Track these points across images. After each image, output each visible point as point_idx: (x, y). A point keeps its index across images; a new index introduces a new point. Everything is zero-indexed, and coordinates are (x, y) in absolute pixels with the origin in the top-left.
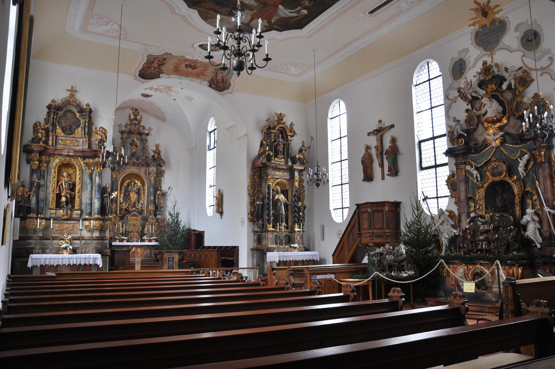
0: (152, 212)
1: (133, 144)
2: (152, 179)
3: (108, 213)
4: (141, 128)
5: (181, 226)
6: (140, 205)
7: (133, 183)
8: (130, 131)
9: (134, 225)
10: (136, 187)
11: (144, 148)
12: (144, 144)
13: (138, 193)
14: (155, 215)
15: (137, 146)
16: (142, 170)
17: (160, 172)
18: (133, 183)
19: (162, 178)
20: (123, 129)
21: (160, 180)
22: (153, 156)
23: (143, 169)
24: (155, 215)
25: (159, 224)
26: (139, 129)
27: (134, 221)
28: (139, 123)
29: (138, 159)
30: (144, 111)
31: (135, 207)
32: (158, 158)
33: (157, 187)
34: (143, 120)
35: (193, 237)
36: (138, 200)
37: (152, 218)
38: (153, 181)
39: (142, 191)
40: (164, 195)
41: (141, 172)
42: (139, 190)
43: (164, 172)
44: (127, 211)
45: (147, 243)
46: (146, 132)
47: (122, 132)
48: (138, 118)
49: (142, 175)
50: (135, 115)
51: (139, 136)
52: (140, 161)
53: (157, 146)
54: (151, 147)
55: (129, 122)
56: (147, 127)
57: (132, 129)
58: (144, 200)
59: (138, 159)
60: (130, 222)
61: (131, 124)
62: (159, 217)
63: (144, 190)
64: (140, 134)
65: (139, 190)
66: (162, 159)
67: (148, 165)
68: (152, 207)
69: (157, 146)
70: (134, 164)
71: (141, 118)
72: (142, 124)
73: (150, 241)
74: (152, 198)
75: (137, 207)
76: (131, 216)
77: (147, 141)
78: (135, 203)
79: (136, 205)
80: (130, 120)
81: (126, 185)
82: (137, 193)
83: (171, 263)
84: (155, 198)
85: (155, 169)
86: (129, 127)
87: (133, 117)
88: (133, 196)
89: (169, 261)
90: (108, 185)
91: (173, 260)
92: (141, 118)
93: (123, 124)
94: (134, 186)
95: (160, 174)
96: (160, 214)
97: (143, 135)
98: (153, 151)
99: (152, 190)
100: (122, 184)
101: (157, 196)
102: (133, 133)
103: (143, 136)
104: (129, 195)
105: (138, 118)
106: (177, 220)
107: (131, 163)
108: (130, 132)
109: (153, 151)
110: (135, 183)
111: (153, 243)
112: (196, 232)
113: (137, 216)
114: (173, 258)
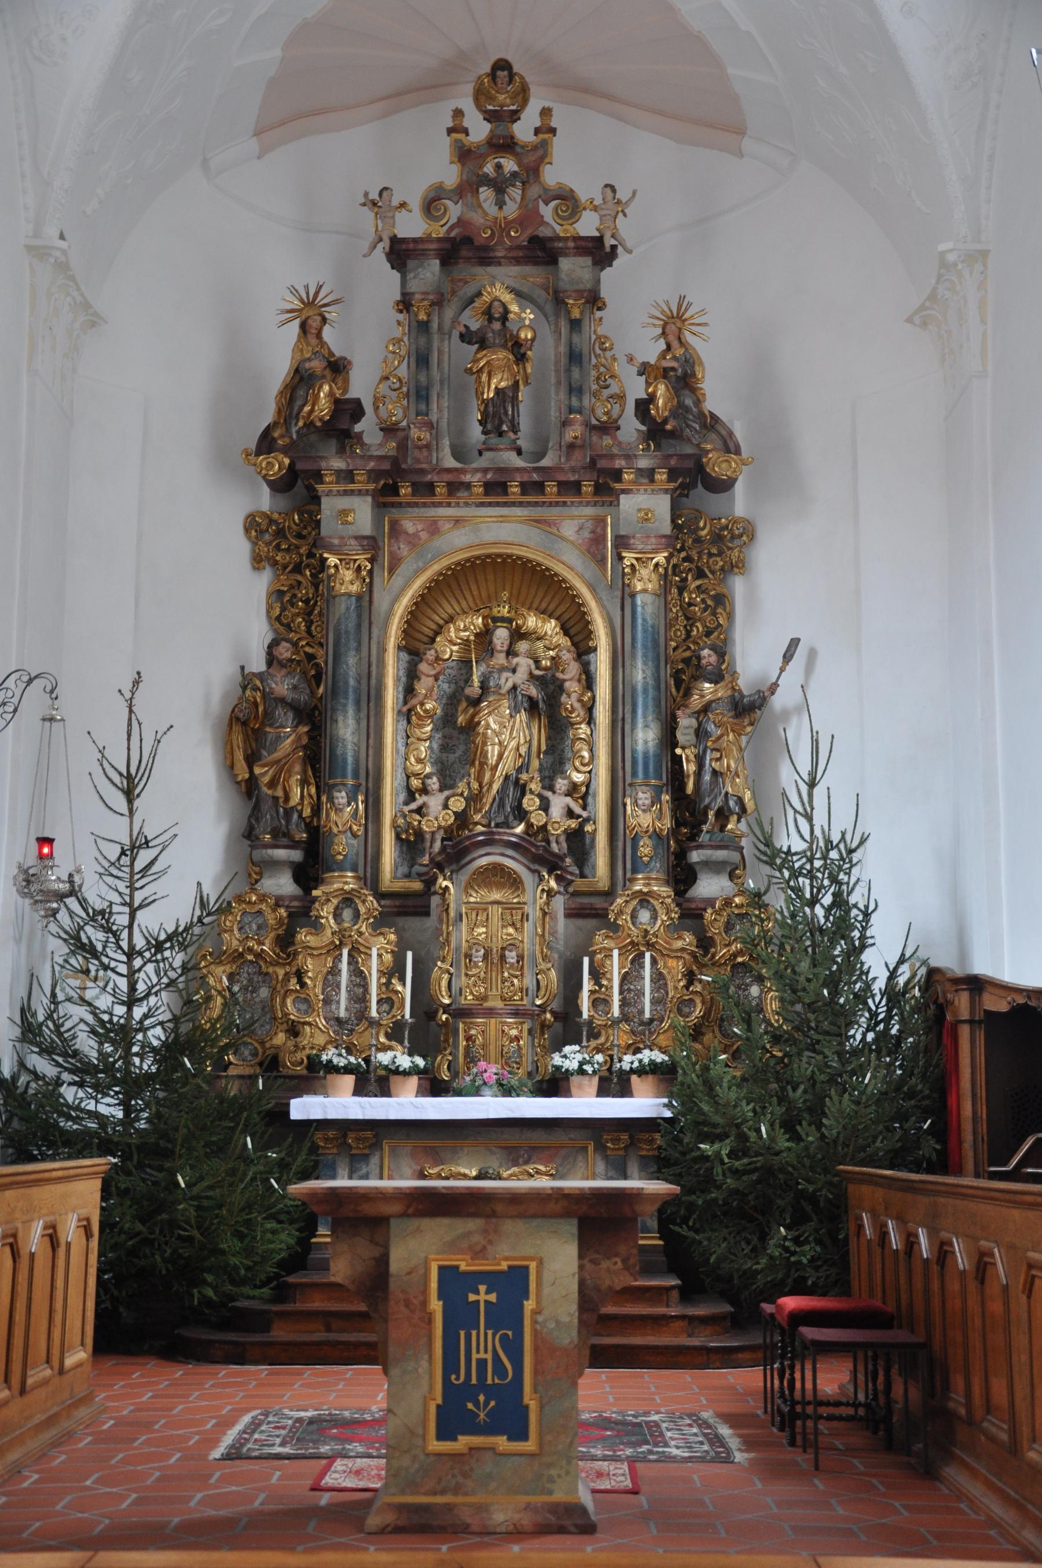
0: (645, 848)
1: (494, 332)
2: (645, 582)
4: (547, 211)
5: (876, 963)
6: (559, 804)
7: (501, 636)
8: (467, 240)
9: (495, 958)
10: (524, 663)
11: (575, 357)
12: (575, 325)
13: (546, 705)
14: (682, 876)
15: (518, 351)
16: (568, 529)
17: (717, 538)
18: (501, 636)
19: (738, 586)
20: (412, 225)
21: (721, 600)
22: (643, 407)
23: (573, 522)
24: (682, 876)
25: (705, 943)
26: (529, 216)
27: (499, 928)
28: (531, 173)
30: (584, 91)
31: (521, 814)
32: (679, 411)
33: (690, 656)
34: (558, 145)
35: (969, 1053)
36: (555, 756)
37: (644, 900)
38: (646, 605)
39: (571, 701)
40: (748, 708)
41: (558, 540)
43: (747, 532)
44: (456, 849)
45: (584, 1104)
46: (587, 225)
47: (401, 254)
48: (524, 130)
49: (570, 565)
50: (491, 117)
51: (533, 275)
52: (546, 462)
53: (674, 324)
54: (629, 332)
55: (450, 175)
56: (587, 190)
57: (477, 219)
58: (593, 762)
60: (461, 935)
61: (467, 189)
62: (710, 887)
63: (589, 682)
64: (542, 252)
66: (711, 423)
67: (606, 485)
68: (647, 814)
69: (674, 324)
70: (496, 488)
71: (545, 130)
72: (552, 176)
73: (613, 1083)
74: (645, 736)
75: (538, 819)
76: (469, 886)
77: (594, 300)
79: (530, 803)
80: (464, 154)
81: (448, 648)
82: (533, 707)
83: (483, 1345)
84: (669, 739)
85: (660, 505)
86: (454, 211)
87: (479, 130)
88: (507, 736)
89: (459, 1318)
91: (507, 1315)
92: (545, 130)
93: (412, 191)
95: (706, 557)
96: (715, 867)
97: (565, 258)
98: (644, 369)
99: (640, 673)
100: (414, 648)
101: (686, 723)
102: (485, 257)
103: (566, 264)
104: (472, 726)
105: (524, 130)
106: (840, 902)
107: (475, 479)
108: (459, 250)
109: (644, 369)
110: (518, 635)
111: (643, 1104)
112: (1000, 1005)
113: (514, 882)
114: (514, 1283)
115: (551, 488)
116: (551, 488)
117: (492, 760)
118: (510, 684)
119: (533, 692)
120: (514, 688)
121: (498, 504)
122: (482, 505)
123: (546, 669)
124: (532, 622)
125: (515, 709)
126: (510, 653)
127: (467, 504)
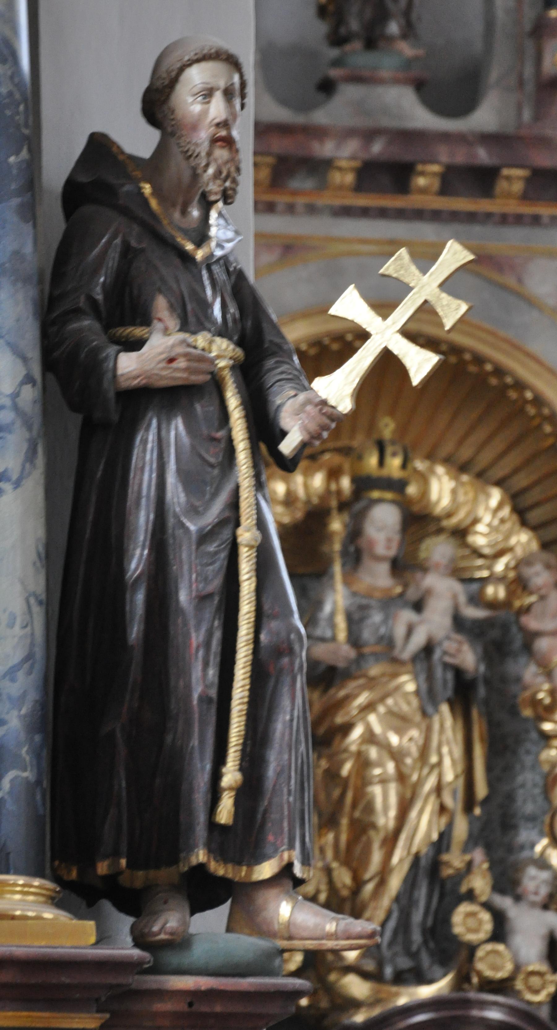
3: (244, 838)
7: (384, 521)
10: (443, 591)
18: (384, 521)
29: (453, 90)
42: (499, 634)
52: (486, 117)
59: (453, 90)
65: (499, 634)
78: (434, 878)
82: (462, 693)
90: (199, 101)
94: (404, 566)
107: (345, 155)
110: (418, 521)
115: (514, 179)
116: (514, 179)
117: (386, 818)
118: (419, 640)
119: (468, 658)
120: (428, 649)
121: (382, 213)
122: (346, 212)
123: (492, 605)
124: (441, 489)
125: (429, 698)
126: (404, 566)
127: (312, 210)
